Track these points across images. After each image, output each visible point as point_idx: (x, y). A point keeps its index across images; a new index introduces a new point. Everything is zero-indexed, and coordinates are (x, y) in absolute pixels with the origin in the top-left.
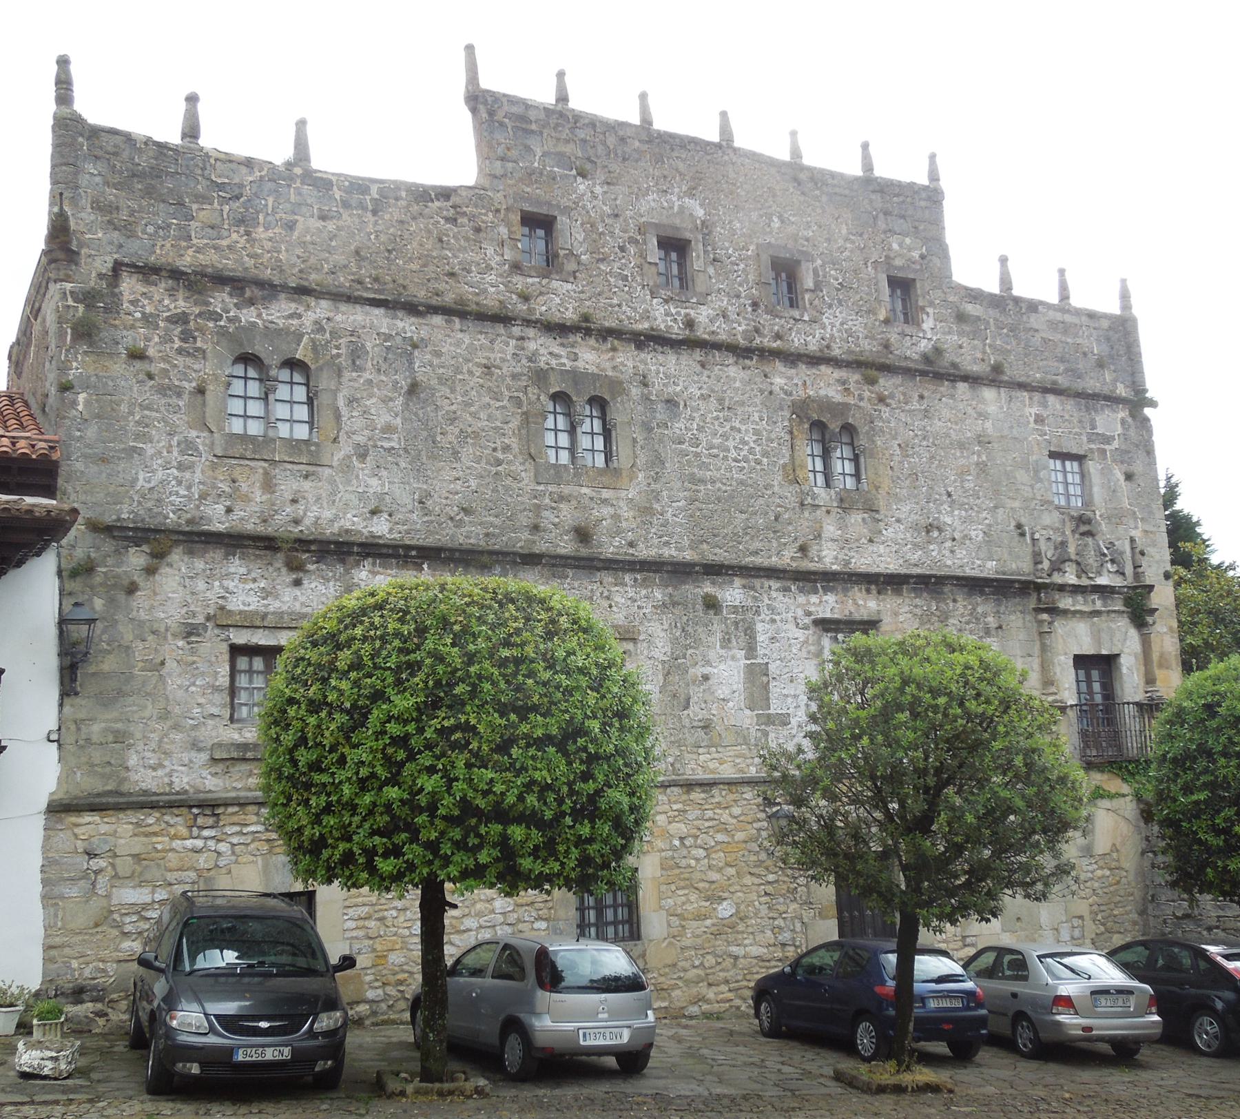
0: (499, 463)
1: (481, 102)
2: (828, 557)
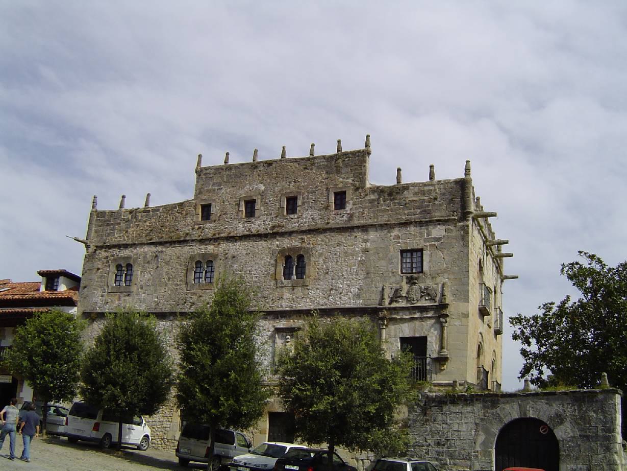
2: (285, 305)
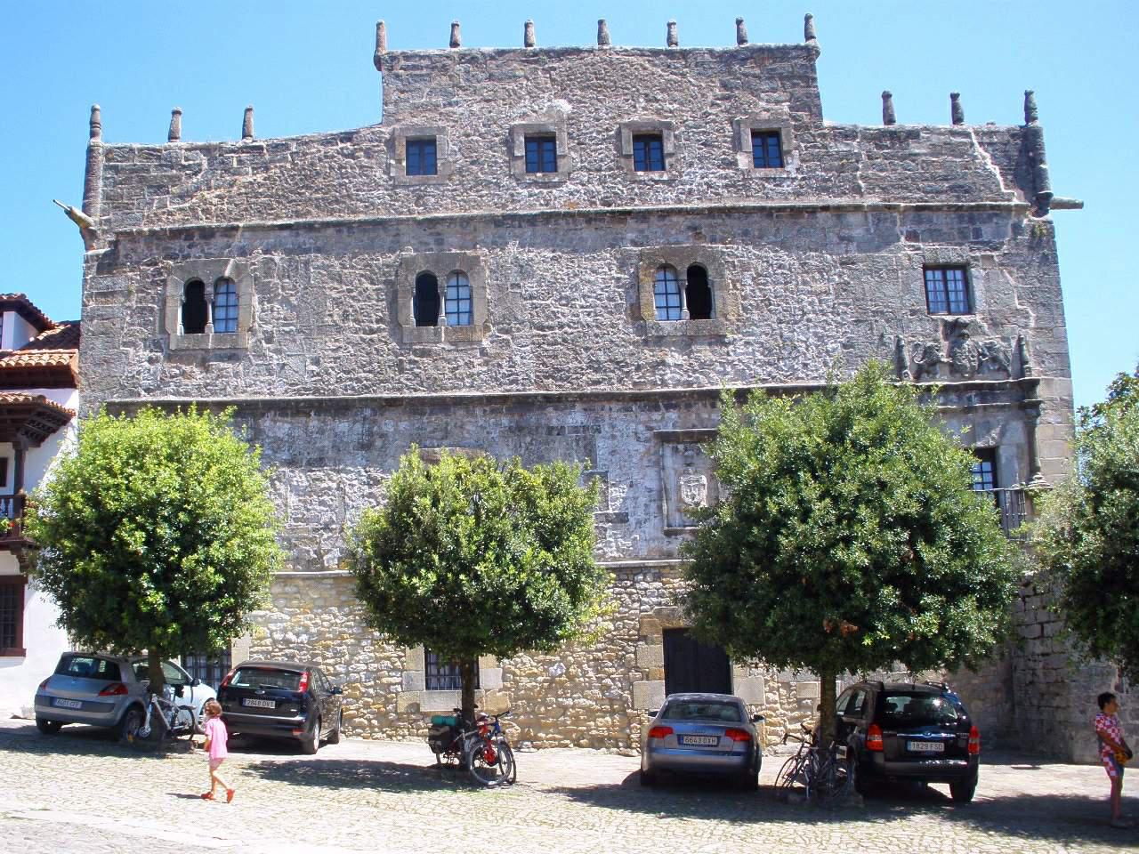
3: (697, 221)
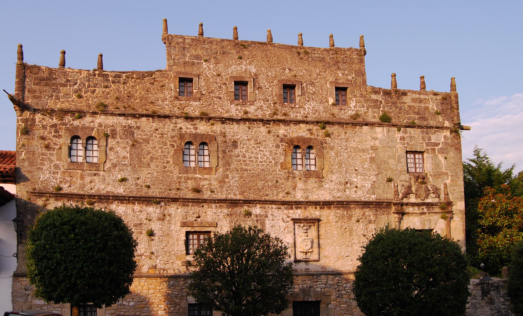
0: (165, 167)
1: (168, 40)
2: (299, 196)
3: (311, 126)
